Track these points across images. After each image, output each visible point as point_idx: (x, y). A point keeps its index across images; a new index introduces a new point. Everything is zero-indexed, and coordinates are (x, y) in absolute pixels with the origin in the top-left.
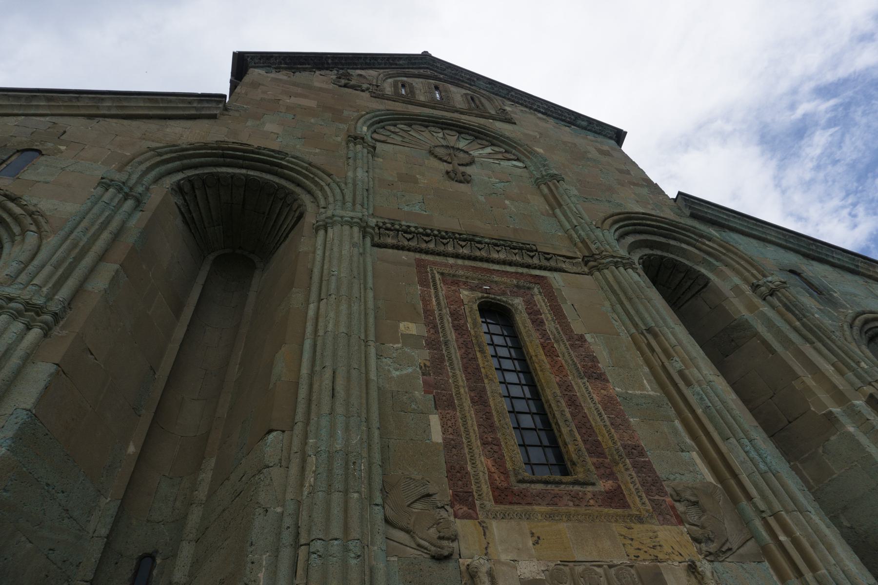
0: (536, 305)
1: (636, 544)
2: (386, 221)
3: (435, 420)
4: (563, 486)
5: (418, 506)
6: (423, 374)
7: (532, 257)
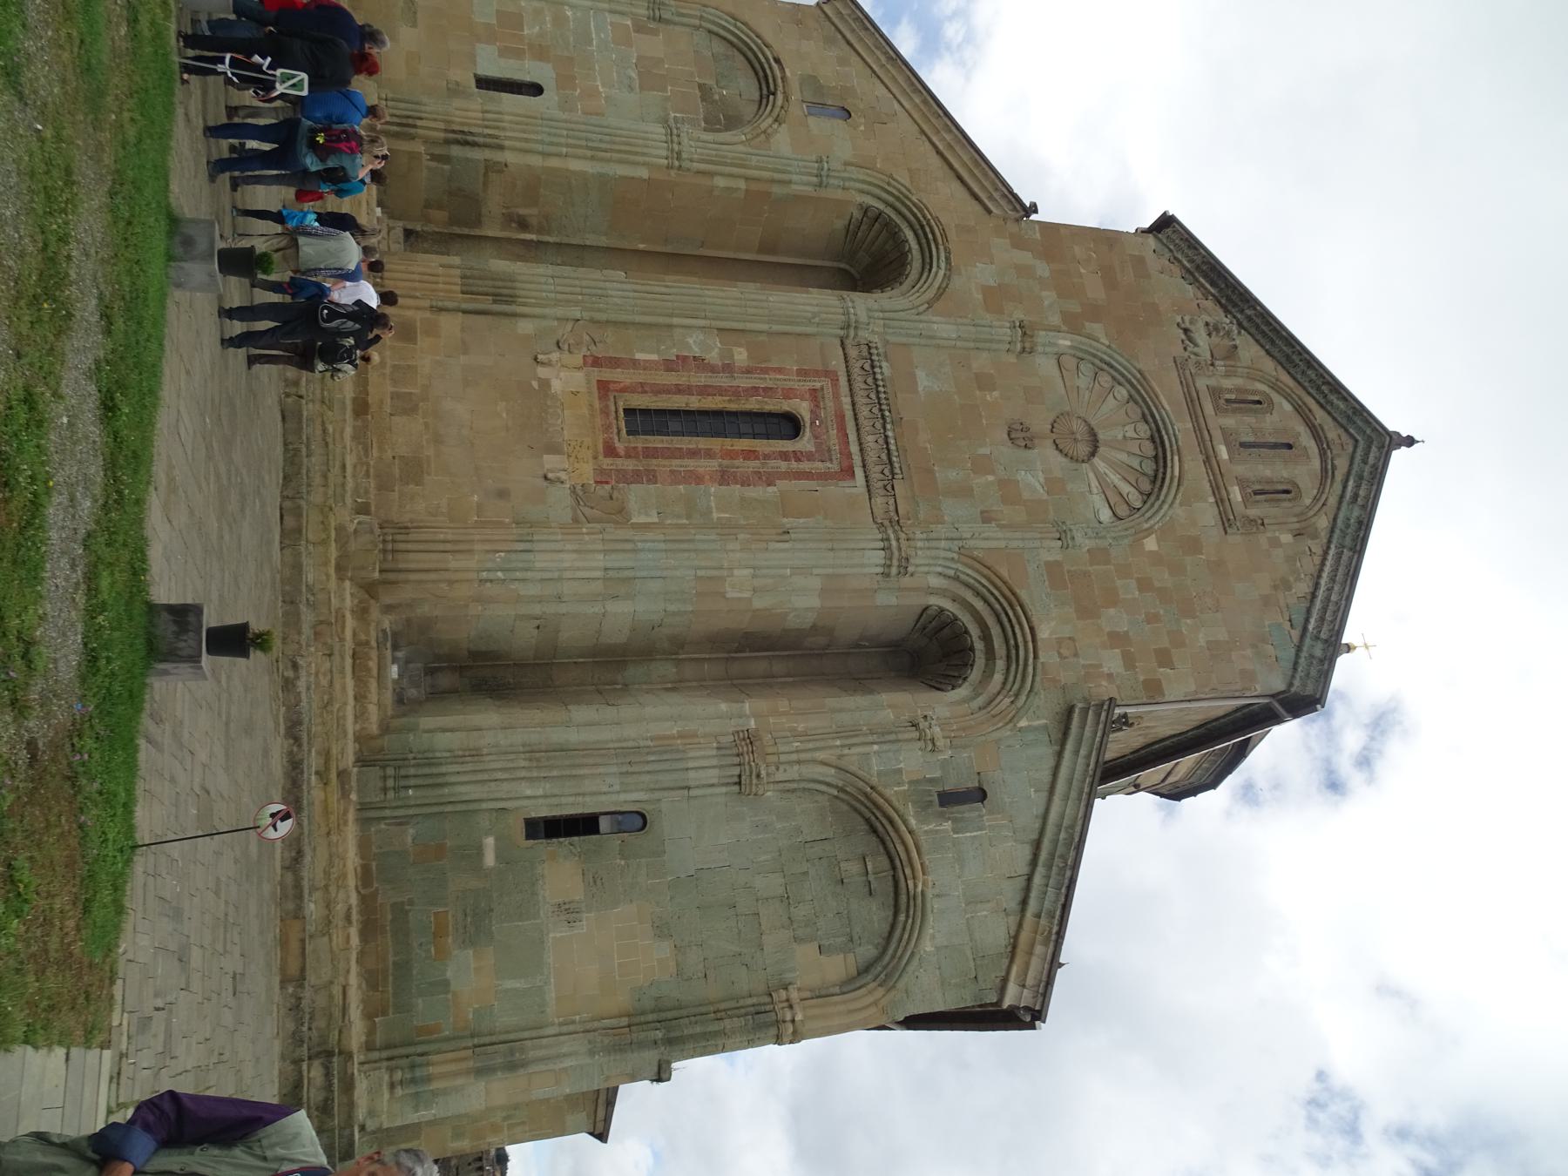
0: (809, 460)
1: (578, 448)
2: (881, 350)
3: (654, 357)
5: (588, 338)
7: (882, 473)
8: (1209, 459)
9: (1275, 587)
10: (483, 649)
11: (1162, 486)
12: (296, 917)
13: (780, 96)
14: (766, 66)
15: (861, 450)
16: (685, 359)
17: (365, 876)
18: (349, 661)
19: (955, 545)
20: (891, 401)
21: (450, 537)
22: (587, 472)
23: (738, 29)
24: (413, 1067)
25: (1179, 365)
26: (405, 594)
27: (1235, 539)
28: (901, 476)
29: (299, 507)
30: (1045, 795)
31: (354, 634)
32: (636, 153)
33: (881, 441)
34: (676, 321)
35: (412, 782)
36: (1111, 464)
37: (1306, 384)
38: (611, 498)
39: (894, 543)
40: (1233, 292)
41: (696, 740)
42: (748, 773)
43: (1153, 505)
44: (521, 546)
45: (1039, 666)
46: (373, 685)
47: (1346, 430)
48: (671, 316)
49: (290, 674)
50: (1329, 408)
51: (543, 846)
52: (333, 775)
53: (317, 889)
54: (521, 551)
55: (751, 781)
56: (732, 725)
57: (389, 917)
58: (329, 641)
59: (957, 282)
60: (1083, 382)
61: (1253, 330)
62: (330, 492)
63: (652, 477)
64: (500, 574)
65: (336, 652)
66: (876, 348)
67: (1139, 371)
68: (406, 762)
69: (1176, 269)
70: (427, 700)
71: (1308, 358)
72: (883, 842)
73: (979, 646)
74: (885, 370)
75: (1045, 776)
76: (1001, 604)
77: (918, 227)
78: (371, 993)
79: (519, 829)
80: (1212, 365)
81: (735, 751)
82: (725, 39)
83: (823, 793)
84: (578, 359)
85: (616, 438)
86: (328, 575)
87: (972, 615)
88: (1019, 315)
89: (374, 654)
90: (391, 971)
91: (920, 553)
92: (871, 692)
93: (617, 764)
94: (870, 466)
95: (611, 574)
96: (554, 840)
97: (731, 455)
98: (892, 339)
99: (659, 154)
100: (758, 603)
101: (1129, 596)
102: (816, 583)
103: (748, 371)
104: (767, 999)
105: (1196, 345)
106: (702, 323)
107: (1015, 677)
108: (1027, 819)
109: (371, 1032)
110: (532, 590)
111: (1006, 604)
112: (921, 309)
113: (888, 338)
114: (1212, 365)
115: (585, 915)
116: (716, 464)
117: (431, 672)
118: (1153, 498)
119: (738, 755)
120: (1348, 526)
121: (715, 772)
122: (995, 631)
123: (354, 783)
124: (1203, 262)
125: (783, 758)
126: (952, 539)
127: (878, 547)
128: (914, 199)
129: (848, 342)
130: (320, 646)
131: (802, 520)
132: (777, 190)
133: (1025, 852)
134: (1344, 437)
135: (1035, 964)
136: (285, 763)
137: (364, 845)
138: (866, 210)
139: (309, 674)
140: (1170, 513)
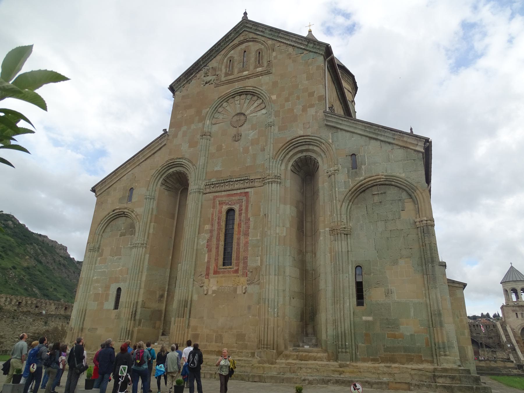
0: (242, 207)
1: (235, 282)
2: (208, 181)
3: (207, 255)
4: (227, 269)
6: (207, 242)
8: (247, 78)
9: (290, 58)
10: (300, 316)
11: (255, 93)
12: (388, 384)
13: (125, 210)
14: (115, 214)
15: (239, 189)
16: (207, 245)
17: (375, 360)
18: (303, 362)
19: (272, 160)
20: (224, 179)
21: (263, 326)
22: (243, 279)
23: (103, 223)
24: (439, 348)
25: (217, 86)
26: (281, 341)
27: (274, 70)
28: (248, 177)
29: (252, 376)
30: (354, 135)
31: (294, 360)
32: (141, 258)
33: (237, 183)
34: (195, 248)
35: (344, 343)
36: (248, 108)
37: (225, 46)
38: (252, 272)
39: (270, 180)
40: (195, 68)
41: (332, 248)
42: (344, 231)
43: (261, 96)
44: (267, 302)
45: (312, 135)
46: (311, 354)
47: (241, 34)
48: (193, 249)
49: (307, 382)
50: (233, 39)
51: (366, 300)
52: (341, 369)
53: (379, 376)
54: (268, 303)
55: (346, 230)
56: (328, 236)
57: (389, 353)
58: (296, 368)
59: (187, 156)
60: (221, 117)
61: (207, 62)
62: (247, 365)
63: (246, 258)
64: (276, 310)
65: (300, 366)
66: (207, 183)
67: (219, 99)
68: (337, 345)
69: (187, 85)
70: (316, 336)
71: (217, 45)
72: (368, 188)
73: (304, 154)
74: (214, 180)
75: (348, 134)
76: (291, 146)
77: (169, 168)
78: (414, 361)
79: (360, 308)
80: (218, 75)
81: (336, 235)
82: (106, 228)
83: (351, 207)
84: (206, 281)
85: (232, 269)
86: (274, 367)
87: (294, 156)
88: (199, 136)
89: (301, 353)
90: (407, 354)
91: (273, 172)
92: (318, 190)
93: (339, 274)
94: (245, 186)
95: (276, 273)
96: (364, 297)
97: (239, 232)
98: (204, 178)
99: (141, 251)
100: (288, 225)
101: (291, 105)
102: (282, 206)
103: (212, 225)
104: (419, 229)
105: (211, 80)
106: (196, 239)
107: (316, 143)
108: (362, 141)
109: (427, 361)
110: (281, 299)
111: (291, 145)
112: (195, 168)
113: (204, 179)
114: (218, 75)
115: (389, 288)
116: (242, 237)
117: (307, 335)
118: (259, 96)
119: (338, 234)
120: (271, 34)
121: (343, 242)
122: (300, 148)
123: (344, 363)
124: (185, 77)
125: (339, 220)
126: (270, 161)
127: (271, 185)
128: (160, 169)
129: (205, 192)
130: (298, 371)
131: (261, 209)
132: (155, 213)
133: (373, 142)
134: (242, 34)
135: (410, 140)
136: (336, 385)
137: (364, 360)
138: (162, 184)
139: (307, 376)
140: (264, 90)
